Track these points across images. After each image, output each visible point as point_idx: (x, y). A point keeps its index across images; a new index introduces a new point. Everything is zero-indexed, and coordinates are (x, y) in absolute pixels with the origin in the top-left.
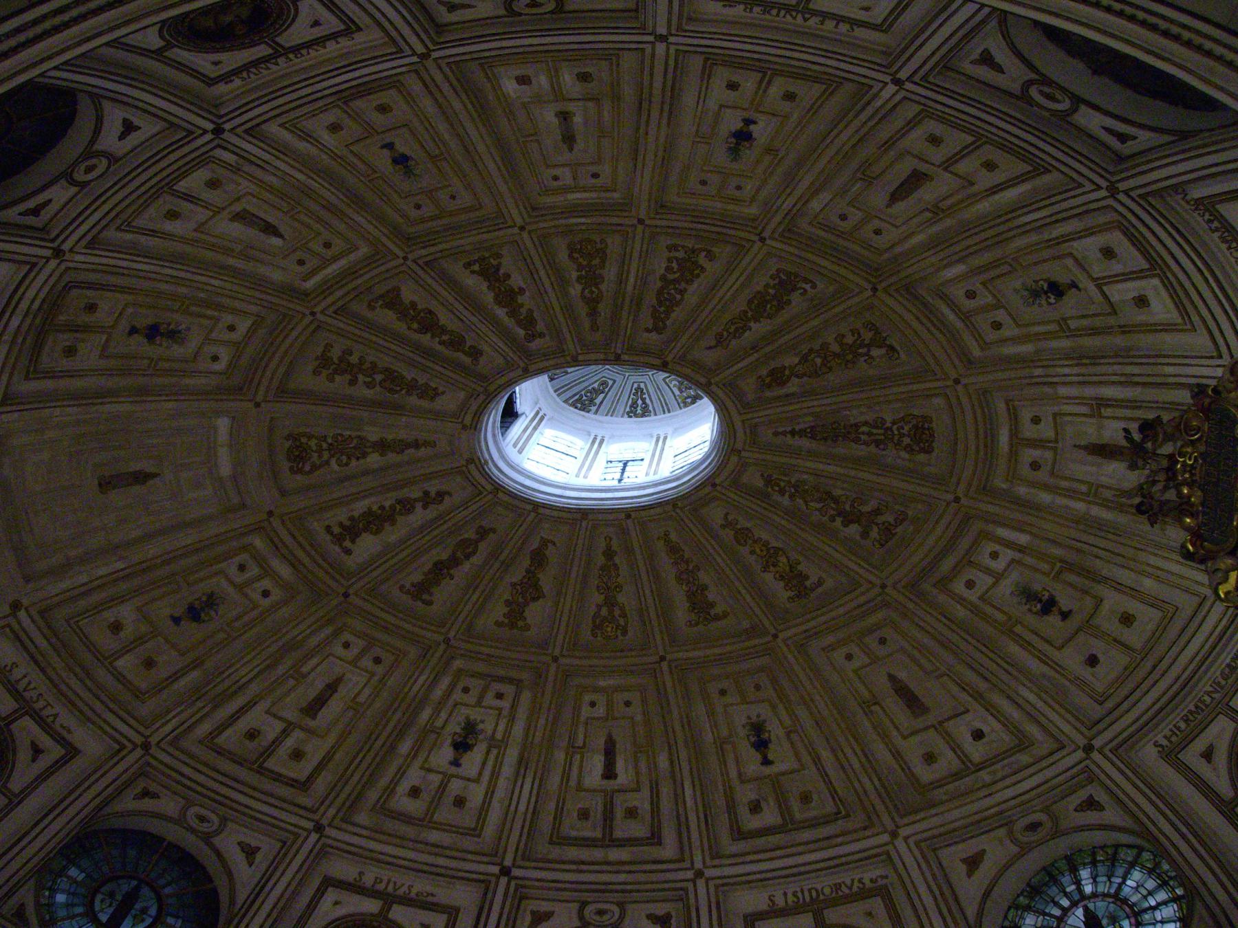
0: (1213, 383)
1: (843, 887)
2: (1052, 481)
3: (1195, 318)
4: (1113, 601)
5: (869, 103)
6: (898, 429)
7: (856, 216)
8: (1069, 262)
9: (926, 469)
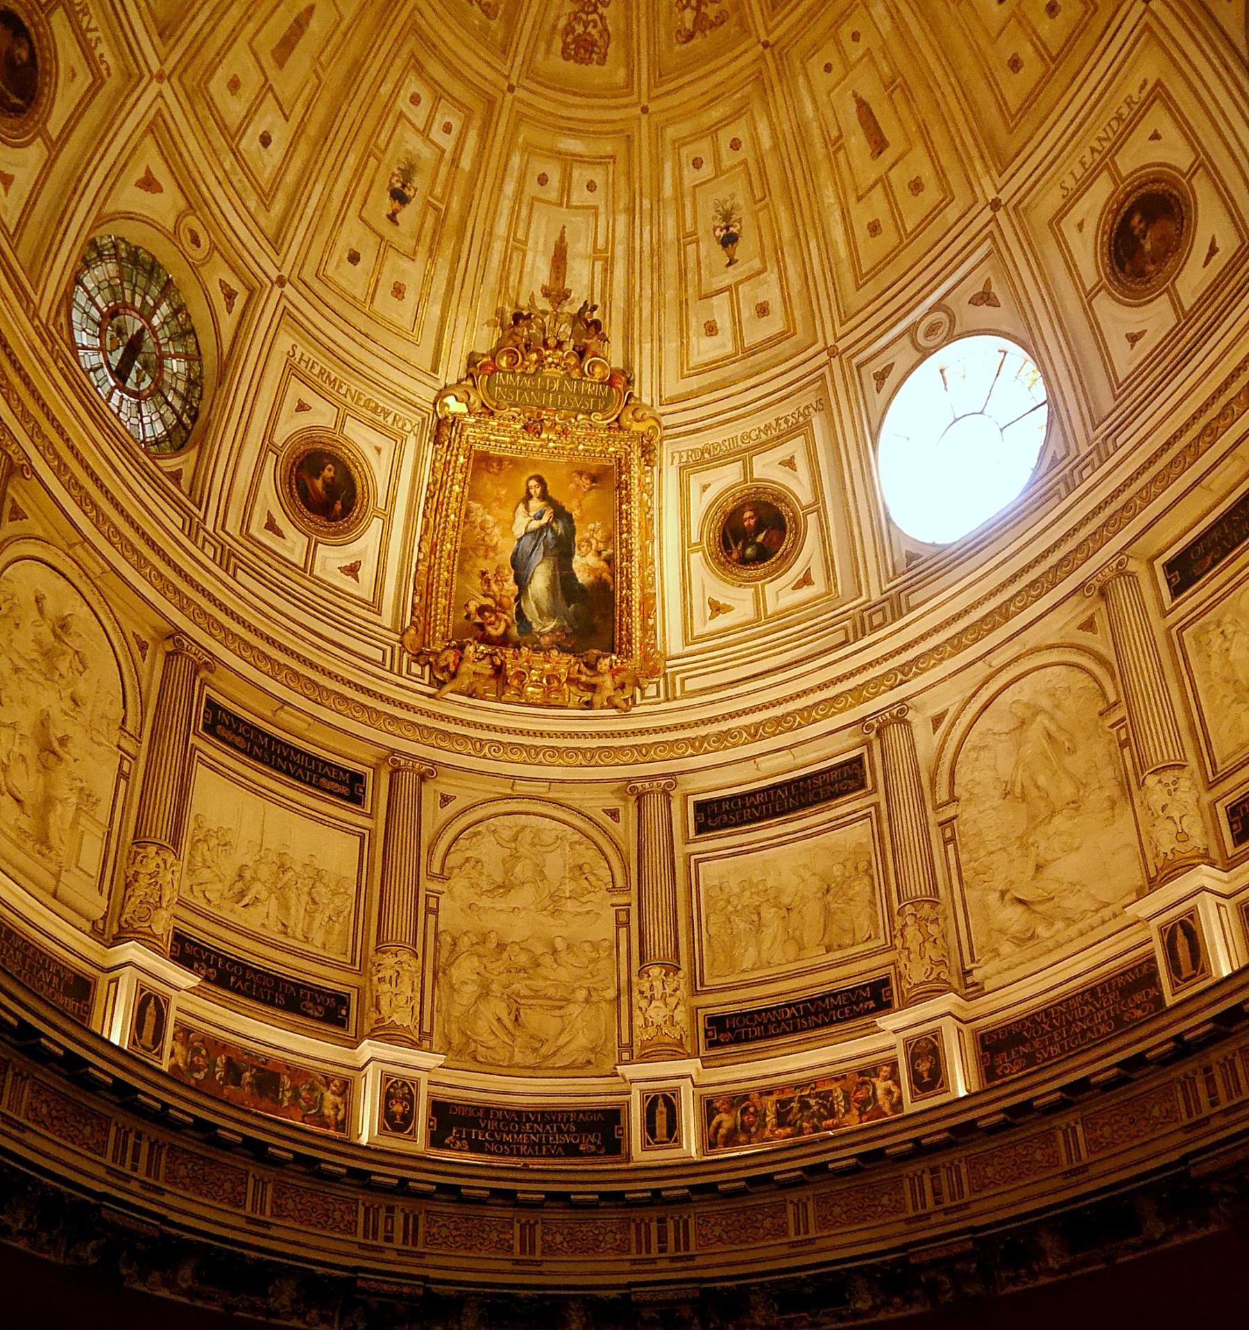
0: (636, 394)
1: (86, 19)
2: (526, 199)
3: (694, 383)
4: (412, 272)
5: (982, 157)
6: (594, 21)
7: (855, 51)
8: (756, 264)
9: (542, 47)
